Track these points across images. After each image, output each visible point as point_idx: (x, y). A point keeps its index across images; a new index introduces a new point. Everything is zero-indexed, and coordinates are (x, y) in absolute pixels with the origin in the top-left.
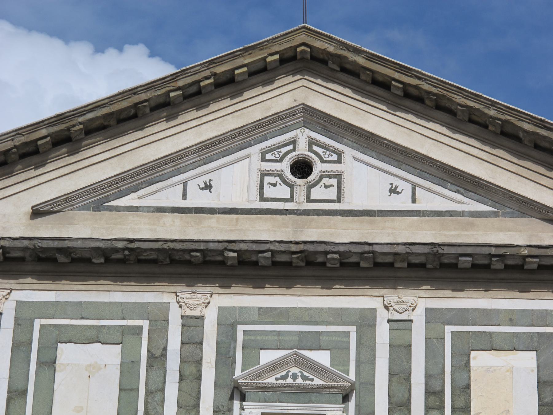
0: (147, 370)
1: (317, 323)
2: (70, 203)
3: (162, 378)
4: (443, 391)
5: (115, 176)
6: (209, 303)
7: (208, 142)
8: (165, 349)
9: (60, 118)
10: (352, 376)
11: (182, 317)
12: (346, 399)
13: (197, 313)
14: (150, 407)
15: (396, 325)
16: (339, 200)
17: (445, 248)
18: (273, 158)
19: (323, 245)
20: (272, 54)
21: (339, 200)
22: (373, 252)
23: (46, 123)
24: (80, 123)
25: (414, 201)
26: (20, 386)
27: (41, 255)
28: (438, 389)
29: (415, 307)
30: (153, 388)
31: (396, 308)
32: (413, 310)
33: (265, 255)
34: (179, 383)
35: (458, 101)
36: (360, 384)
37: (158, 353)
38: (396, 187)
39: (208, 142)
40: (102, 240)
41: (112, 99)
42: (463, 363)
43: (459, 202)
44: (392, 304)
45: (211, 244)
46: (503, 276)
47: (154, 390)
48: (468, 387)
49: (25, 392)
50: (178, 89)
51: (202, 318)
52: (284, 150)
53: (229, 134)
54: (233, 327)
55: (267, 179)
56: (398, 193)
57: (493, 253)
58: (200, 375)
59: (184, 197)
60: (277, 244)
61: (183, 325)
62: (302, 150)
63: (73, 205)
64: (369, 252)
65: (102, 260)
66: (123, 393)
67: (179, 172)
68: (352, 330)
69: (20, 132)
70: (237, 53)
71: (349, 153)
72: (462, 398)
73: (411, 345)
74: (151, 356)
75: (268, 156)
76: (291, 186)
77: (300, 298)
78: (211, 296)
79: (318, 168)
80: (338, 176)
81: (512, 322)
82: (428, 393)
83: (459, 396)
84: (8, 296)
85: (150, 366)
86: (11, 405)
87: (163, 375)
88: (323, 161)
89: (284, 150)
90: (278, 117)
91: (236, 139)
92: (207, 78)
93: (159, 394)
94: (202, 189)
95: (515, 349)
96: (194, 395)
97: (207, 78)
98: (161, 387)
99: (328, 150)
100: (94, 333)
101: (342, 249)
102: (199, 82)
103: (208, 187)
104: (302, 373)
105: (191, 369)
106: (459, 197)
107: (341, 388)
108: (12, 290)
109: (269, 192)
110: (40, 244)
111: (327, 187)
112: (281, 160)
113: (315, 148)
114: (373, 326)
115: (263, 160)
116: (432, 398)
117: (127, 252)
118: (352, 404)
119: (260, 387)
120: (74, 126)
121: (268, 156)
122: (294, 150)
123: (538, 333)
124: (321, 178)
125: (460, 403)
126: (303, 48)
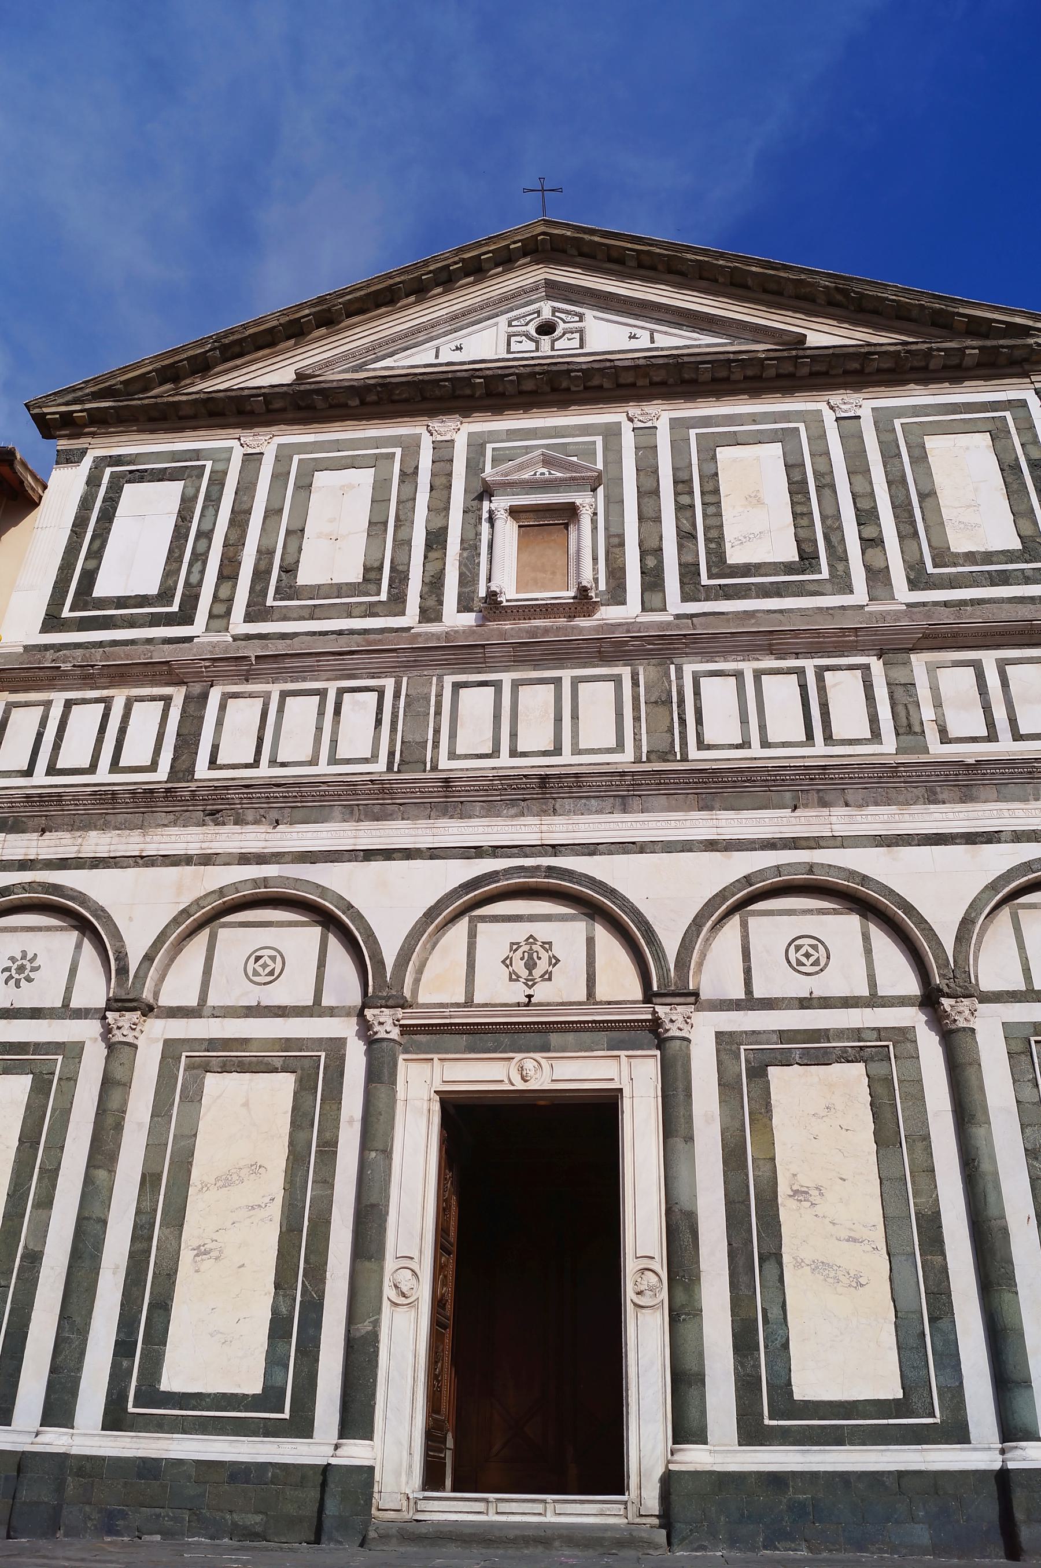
0: (399, 485)
1: (563, 437)
2: (331, 367)
3: (414, 490)
4: (691, 480)
5: (372, 342)
6: (459, 429)
7: (458, 312)
8: (417, 468)
9: (321, 300)
10: (600, 466)
11: (433, 442)
12: (594, 490)
13: (447, 438)
14: (401, 513)
15: (641, 432)
16: (581, 347)
17: (685, 358)
18: (519, 324)
19: (566, 365)
20: (515, 242)
21: (581, 347)
22: (615, 367)
23: (308, 304)
24: (340, 303)
25: (652, 342)
26: (277, 507)
27: (301, 403)
28: (686, 478)
29: (659, 416)
30: (404, 498)
31: (641, 418)
32: (657, 419)
33: (510, 378)
34: (430, 492)
35: (689, 257)
36: (608, 480)
37: (410, 471)
38: (635, 335)
39: (458, 312)
40: (356, 379)
41: (369, 282)
42: (709, 457)
43: (696, 340)
44: (636, 416)
45: (458, 373)
46: (743, 386)
47: (405, 500)
48: (717, 474)
49: (281, 510)
50: (430, 272)
51: (453, 441)
52: (529, 318)
53: (477, 305)
54: (482, 447)
55: (513, 339)
56: (637, 338)
57: (732, 358)
58: (451, 485)
59: (437, 357)
60: (522, 368)
61: (434, 448)
62: (547, 314)
63: (333, 369)
64: (610, 368)
65: (357, 402)
66: (375, 504)
67: (432, 339)
68: (599, 440)
69: (285, 312)
70: (483, 242)
71: (589, 314)
72: (711, 484)
73: (656, 447)
74: (403, 474)
75: (514, 323)
76: (537, 342)
77: (546, 419)
78: (461, 423)
79: (561, 327)
80: (581, 332)
81: (755, 422)
82: (676, 482)
83: (708, 482)
84: (270, 441)
85: (402, 481)
86: (267, 521)
87: (414, 488)
88: (565, 322)
89: (529, 318)
90: (523, 291)
91: (484, 310)
92: (456, 263)
93: (411, 502)
94: (454, 350)
95: (760, 443)
96: (445, 499)
97: (456, 263)
98: (412, 496)
99: (570, 314)
100: (349, 461)
101: (584, 367)
102: (449, 265)
103: (459, 348)
104: (550, 472)
105: (441, 481)
106: (695, 335)
107: (588, 478)
108: (273, 436)
109: (514, 347)
110: (298, 388)
111: (569, 339)
112: (527, 324)
113: (557, 314)
114: (619, 434)
115: (510, 325)
116: (680, 486)
117: (379, 389)
118: (601, 490)
119: (508, 483)
120: (335, 306)
121: (514, 323)
122: (539, 316)
123: (782, 429)
124: (564, 334)
125: (709, 487)
126: (542, 237)
